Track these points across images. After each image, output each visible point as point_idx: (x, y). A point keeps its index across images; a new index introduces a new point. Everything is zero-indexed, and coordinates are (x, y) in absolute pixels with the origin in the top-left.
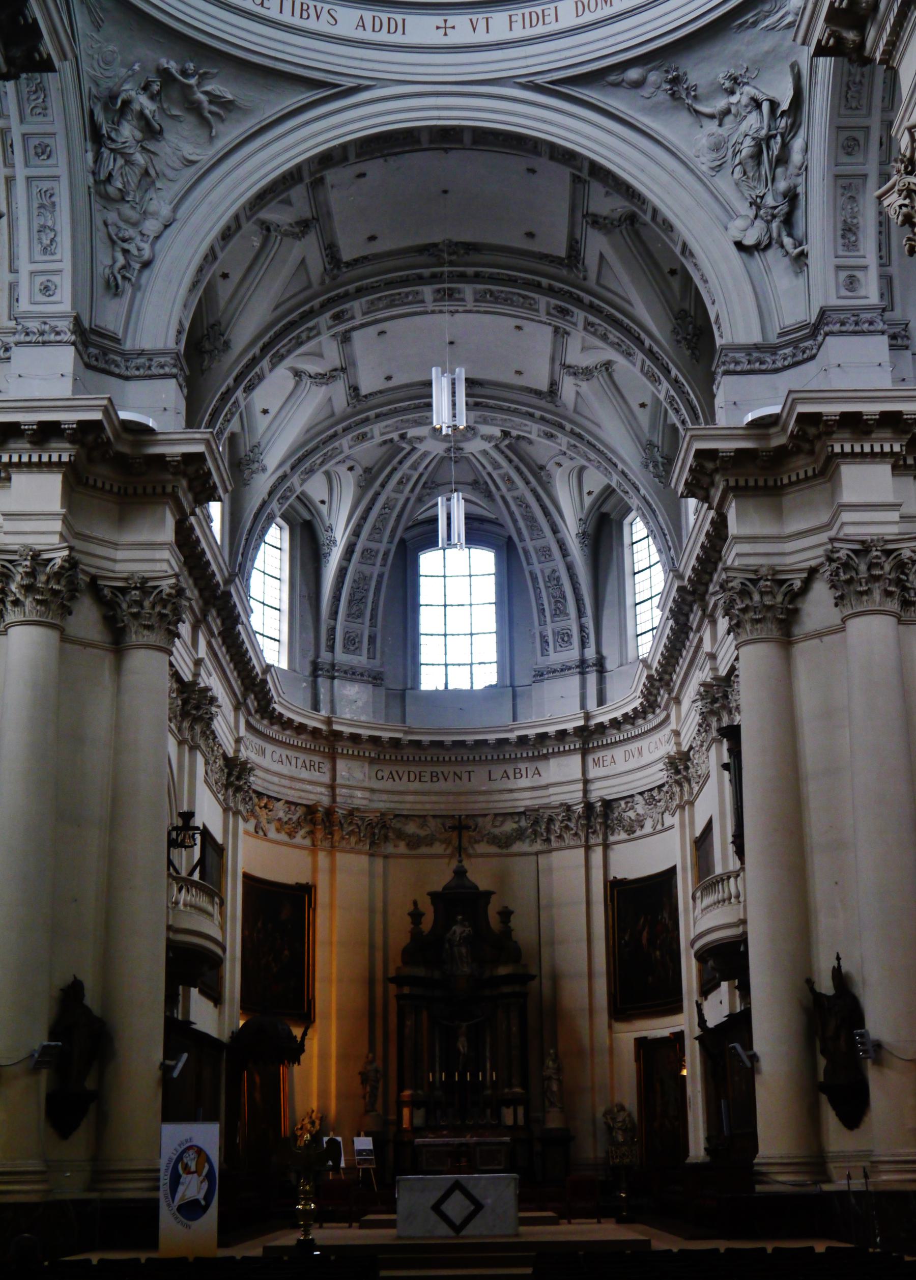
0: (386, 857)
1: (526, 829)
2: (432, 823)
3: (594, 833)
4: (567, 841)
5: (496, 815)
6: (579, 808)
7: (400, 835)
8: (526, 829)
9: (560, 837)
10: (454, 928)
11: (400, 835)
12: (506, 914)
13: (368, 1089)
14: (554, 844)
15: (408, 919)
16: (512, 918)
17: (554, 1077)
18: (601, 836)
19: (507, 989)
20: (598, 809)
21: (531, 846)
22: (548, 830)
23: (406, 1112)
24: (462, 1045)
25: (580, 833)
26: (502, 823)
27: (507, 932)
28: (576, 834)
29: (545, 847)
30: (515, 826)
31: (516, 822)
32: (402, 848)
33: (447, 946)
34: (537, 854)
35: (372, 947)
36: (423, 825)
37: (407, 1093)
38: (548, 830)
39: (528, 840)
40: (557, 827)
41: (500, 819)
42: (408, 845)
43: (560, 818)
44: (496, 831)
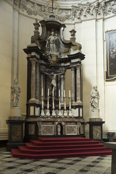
0: (19, 13)
1: (70, 15)
2: (36, 6)
3: (99, 14)
4: (88, 18)
5: (60, 9)
6: (96, 4)
7: (25, 8)
8: (70, 15)
9: (85, 16)
10: (50, 37)
11: (25, 8)
12: (73, 32)
13: (15, 96)
14: (82, 18)
15: (34, 27)
16: (76, 33)
17: (96, 97)
18: (102, 15)
19: (73, 61)
20: (103, 4)
21: (72, 22)
22: (80, 14)
23: (32, 108)
24: (54, 83)
25: (94, 14)
26: (62, 12)
27: (74, 39)
28: (92, 14)
29: (79, 21)
30: (66, 14)
31: (67, 13)
32: (25, 13)
33: (48, 42)
34: (74, 24)
35: (13, 45)
36: (33, 7)
37: (33, 99)
38: (80, 14)
39: (71, 19)
40: (84, 13)
41: (61, 11)
42: (28, 12)
43: (86, 9)
44: (60, 15)
